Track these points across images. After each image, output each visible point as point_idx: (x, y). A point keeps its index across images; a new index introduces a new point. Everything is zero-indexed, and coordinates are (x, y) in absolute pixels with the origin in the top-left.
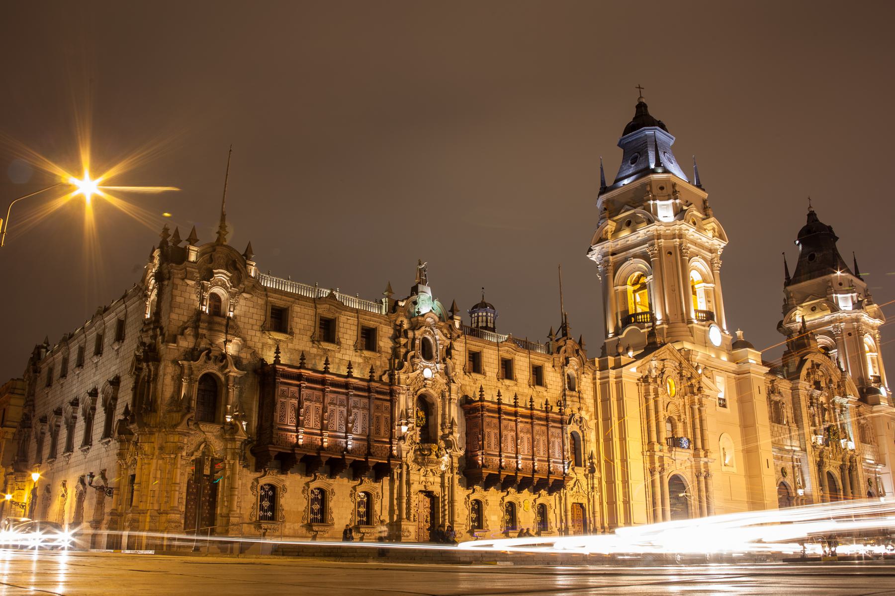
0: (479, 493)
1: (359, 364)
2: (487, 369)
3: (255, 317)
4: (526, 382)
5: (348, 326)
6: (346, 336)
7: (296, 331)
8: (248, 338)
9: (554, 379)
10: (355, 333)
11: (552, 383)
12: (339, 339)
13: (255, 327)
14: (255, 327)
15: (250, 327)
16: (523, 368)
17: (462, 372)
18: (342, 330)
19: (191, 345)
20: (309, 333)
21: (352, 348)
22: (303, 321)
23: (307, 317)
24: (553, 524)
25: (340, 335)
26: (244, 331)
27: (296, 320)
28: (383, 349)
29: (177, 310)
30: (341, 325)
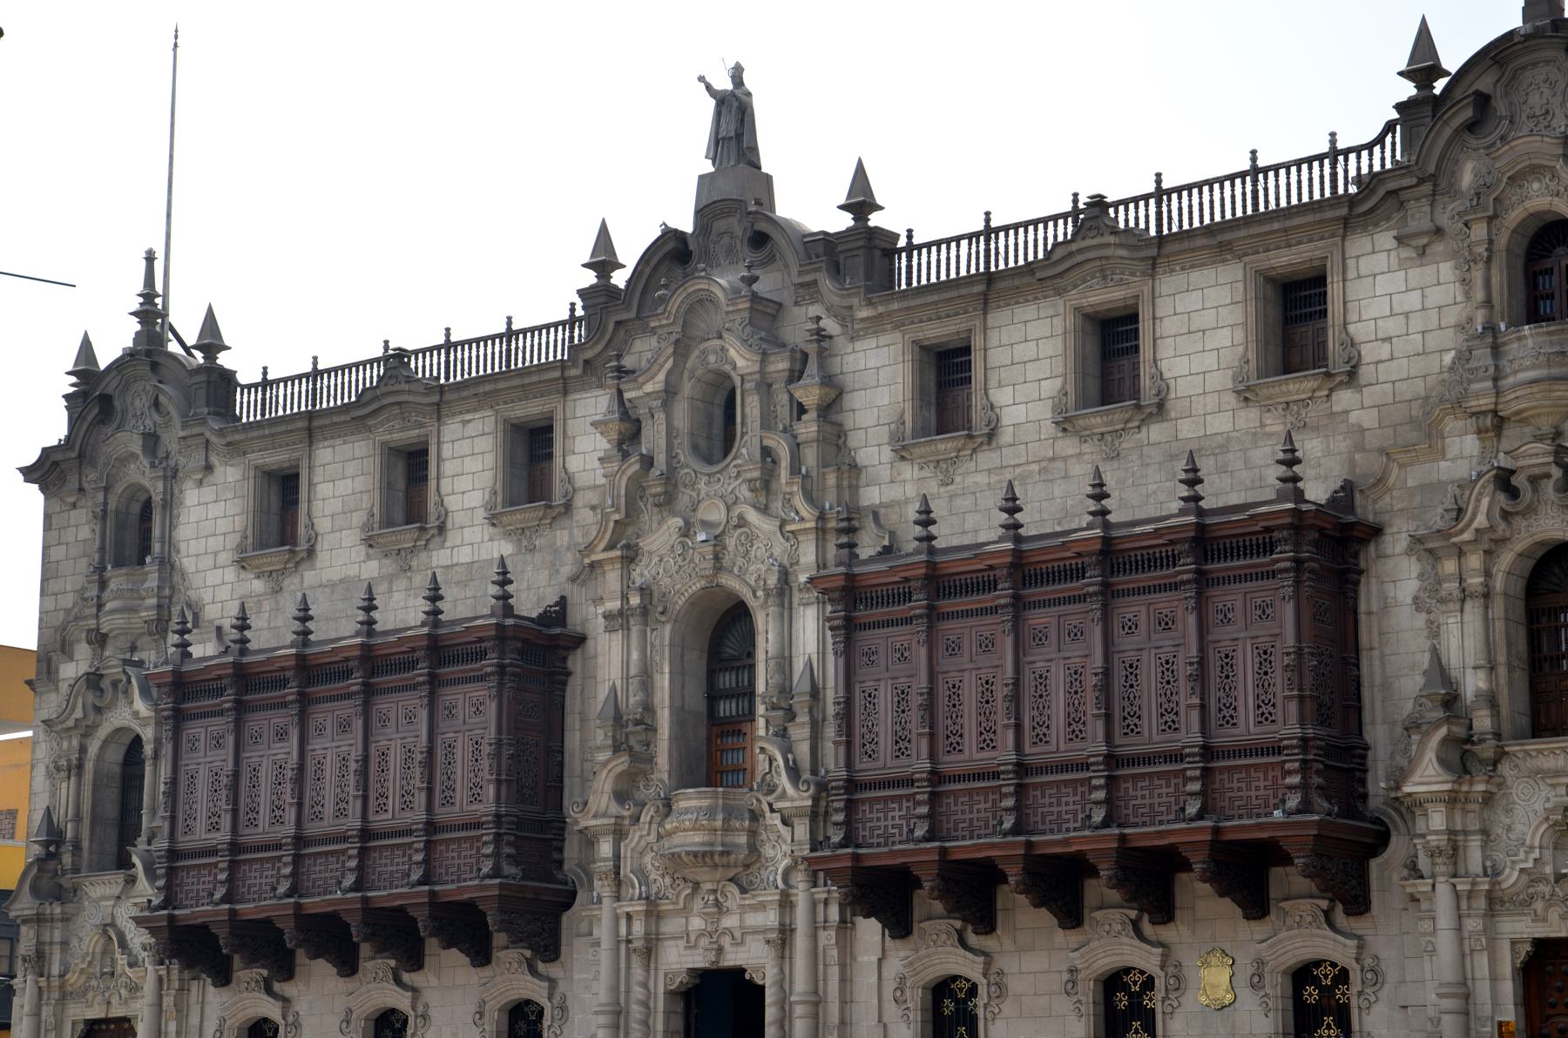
2: (1001, 396)
3: (223, 525)
4: (1222, 380)
7: (323, 525)
8: (207, 597)
10: (490, 460)
11: (1392, 327)
15: (209, 561)
16: (1207, 319)
17: (887, 453)
18: (449, 468)
20: (359, 518)
21: (481, 514)
23: (351, 468)
25: (446, 486)
26: (196, 581)
27: (323, 490)
29: (54, 586)
30: (447, 451)
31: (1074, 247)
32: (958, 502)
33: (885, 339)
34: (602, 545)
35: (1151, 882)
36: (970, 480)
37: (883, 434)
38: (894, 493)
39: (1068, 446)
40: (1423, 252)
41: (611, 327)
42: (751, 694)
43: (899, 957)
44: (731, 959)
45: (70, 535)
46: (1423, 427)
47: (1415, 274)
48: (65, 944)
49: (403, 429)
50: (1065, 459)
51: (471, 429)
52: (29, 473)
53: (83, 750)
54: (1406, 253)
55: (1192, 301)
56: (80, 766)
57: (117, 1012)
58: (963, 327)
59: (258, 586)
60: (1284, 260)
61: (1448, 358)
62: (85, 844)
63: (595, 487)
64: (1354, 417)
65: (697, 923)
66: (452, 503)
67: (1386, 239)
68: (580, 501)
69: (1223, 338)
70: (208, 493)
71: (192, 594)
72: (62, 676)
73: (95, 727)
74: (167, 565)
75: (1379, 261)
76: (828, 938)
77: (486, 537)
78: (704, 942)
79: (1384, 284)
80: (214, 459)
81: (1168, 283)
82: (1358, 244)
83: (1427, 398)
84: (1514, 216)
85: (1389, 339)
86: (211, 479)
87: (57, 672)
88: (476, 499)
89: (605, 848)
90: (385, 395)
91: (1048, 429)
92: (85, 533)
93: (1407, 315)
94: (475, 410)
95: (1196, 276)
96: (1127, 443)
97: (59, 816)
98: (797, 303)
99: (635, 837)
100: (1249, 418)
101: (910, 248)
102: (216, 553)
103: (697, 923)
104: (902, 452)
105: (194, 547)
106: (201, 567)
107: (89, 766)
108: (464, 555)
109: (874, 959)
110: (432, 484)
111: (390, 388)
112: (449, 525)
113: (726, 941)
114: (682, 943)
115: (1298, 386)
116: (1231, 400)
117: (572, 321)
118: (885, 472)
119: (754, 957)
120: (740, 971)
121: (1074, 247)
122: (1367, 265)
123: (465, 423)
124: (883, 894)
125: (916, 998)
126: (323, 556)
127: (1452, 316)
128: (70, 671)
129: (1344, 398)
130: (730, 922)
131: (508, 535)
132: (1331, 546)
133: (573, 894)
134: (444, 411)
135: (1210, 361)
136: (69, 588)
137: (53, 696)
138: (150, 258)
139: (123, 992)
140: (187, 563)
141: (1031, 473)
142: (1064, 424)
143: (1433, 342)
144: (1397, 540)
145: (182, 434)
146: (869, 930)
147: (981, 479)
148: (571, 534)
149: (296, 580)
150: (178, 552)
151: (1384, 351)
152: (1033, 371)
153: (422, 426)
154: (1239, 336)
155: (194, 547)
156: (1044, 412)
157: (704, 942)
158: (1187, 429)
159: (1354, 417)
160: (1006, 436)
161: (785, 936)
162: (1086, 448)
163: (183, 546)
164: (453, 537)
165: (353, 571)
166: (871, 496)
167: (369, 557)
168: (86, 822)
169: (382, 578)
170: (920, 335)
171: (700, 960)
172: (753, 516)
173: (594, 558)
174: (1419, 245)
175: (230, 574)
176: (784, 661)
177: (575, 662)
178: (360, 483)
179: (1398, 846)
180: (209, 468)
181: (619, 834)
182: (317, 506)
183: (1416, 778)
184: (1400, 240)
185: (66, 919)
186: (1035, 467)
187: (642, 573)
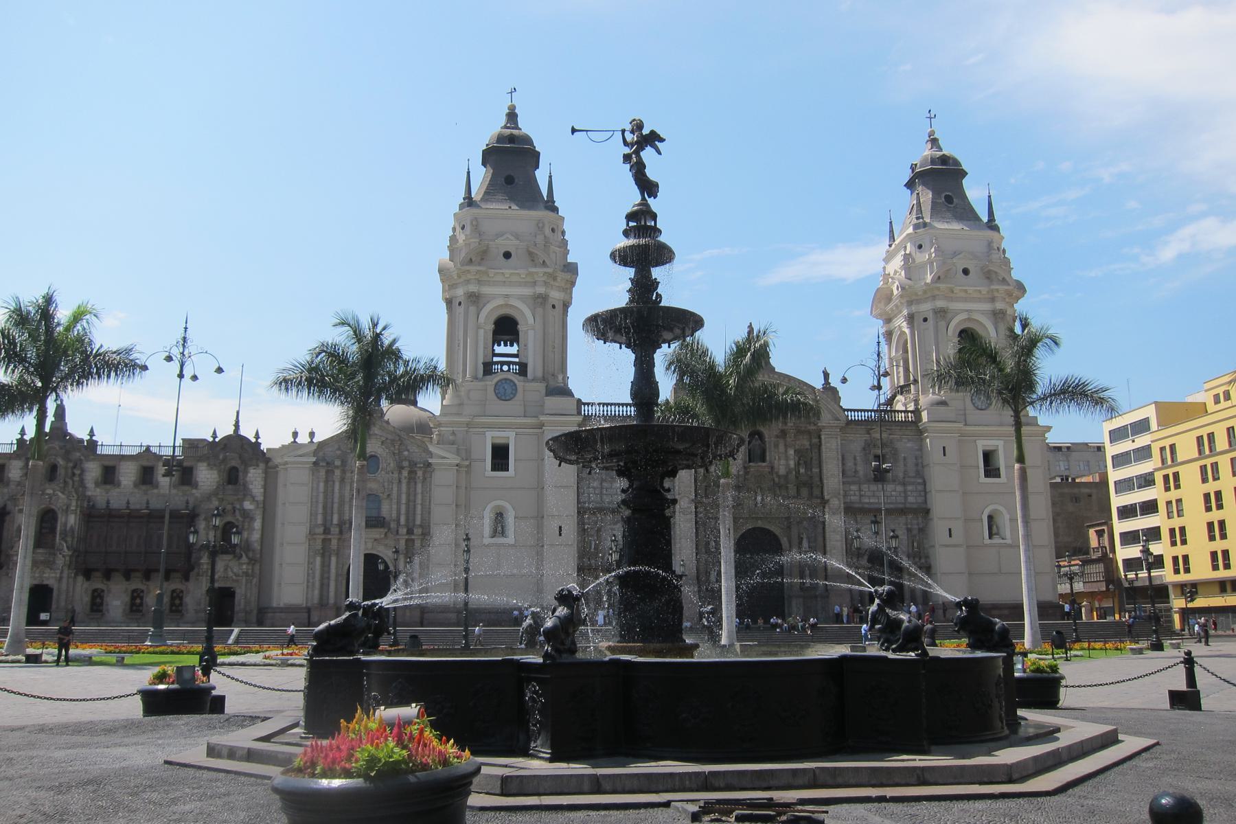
43: (86, 584)
46: (208, 498)
76: (71, 580)
104: (97, 484)
115: (186, 488)
119: (51, 582)
124: (88, 574)
125: (90, 592)
129: (194, 491)
132: (188, 518)
142: (136, 485)
144: (202, 517)
146: (80, 579)
156: (131, 484)
161: (61, 578)
174: (210, 466)
176: (66, 524)
177: (7, 518)
179: (196, 570)
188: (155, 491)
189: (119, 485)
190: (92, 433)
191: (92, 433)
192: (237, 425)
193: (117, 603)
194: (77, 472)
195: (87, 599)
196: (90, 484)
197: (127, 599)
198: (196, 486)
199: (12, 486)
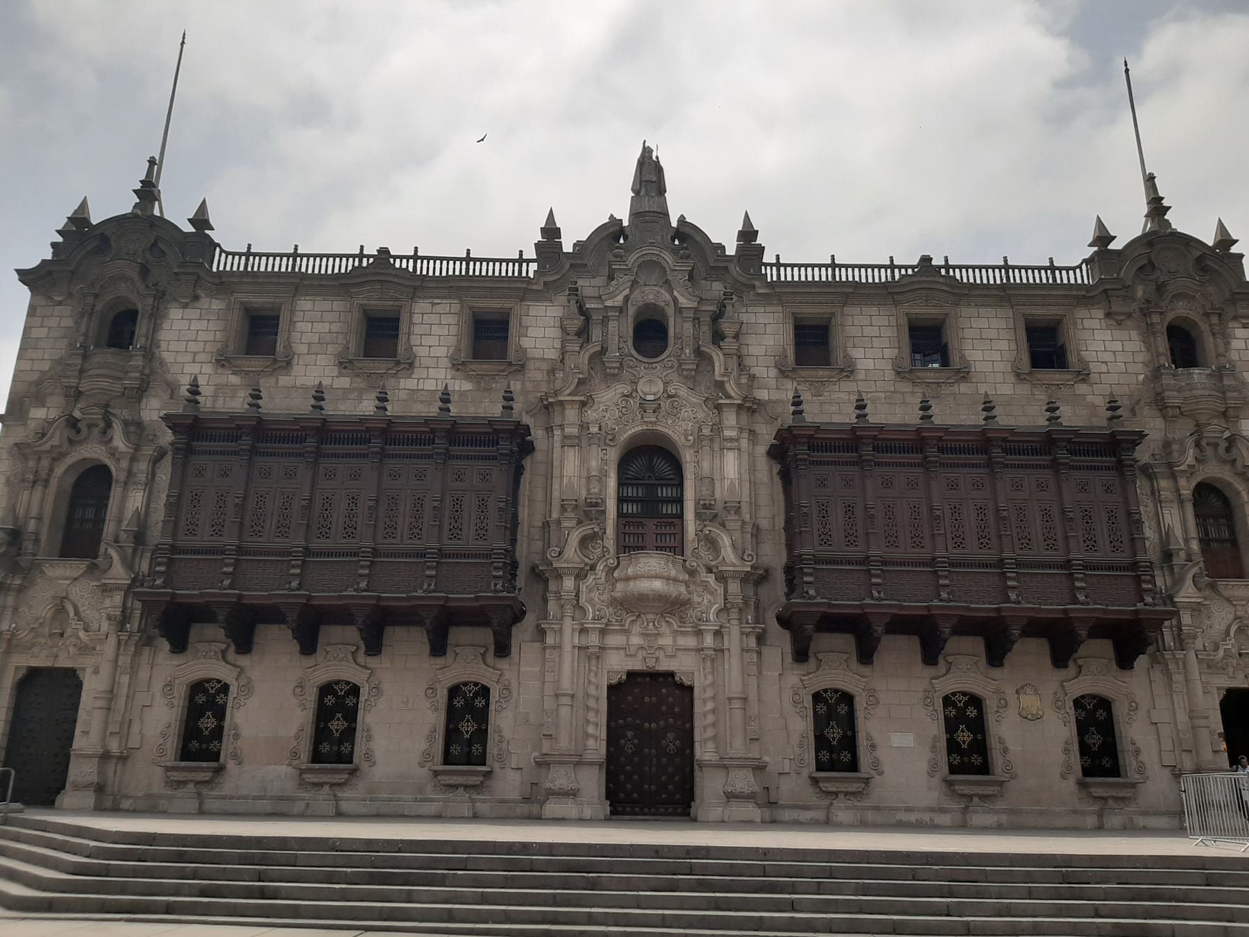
0: (836, 670)
1: (462, 394)
2: (857, 353)
3: (202, 336)
5: (434, 319)
6: (427, 341)
9: (1117, 346)
10: (454, 330)
11: (1108, 357)
12: (410, 348)
13: (201, 357)
14: (201, 357)
15: (189, 358)
16: (992, 334)
17: (773, 372)
18: (417, 329)
19: (53, 414)
20: (331, 348)
21: (445, 362)
22: (319, 327)
23: (329, 317)
24: (1150, 757)
25: (414, 340)
28: (530, 353)
29: (31, 354)
30: (417, 318)
31: (916, 279)
32: (826, 407)
33: (768, 309)
34: (568, 392)
35: (996, 642)
36: (835, 396)
37: (771, 361)
38: (775, 395)
39: (905, 387)
40: (1119, 323)
41: (567, 266)
42: (680, 501)
44: (664, 666)
45: (53, 322)
47: (1117, 333)
48: (15, 610)
49: (380, 299)
50: (903, 393)
51: (438, 309)
52: (25, 276)
53: (51, 470)
54: (1110, 322)
55: (983, 323)
56: (47, 481)
57: (64, 662)
58: (828, 311)
59: (234, 379)
60: (1040, 312)
61: (1141, 378)
62: (43, 538)
63: (543, 359)
64: (1089, 398)
65: (636, 640)
66: (420, 351)
67: (1099, 313)
68: (531, 365)
69: (1004, 345)
70: (192, 313)
71: (169, 377)
72: (31, 416)
73: (62, 456)
74: (150, 353)
75: (1095, 324)
77: (449, 376)
78: (641, 654)
79: (1098, 335)
80: (200, 293)
81: (965, 311)
82: (1081, 313)
83: (1131, 396)
84: (1170, 316)
85: (1106, 363)
86: (196, 305)
87: (27, 412)
88: (442, 352)
89: (569, 583)
90: (377, 274)
91: (890, 374)
92: (69, 322)
93: (1114, 352)
94: (445, 298)
95: (982, 310)
96: (946, 390)
97: (21, 512)
98: (705, 279)
99: (591, 579)
100: (1024, 389)
101: (778, 265)
102: (195, 353)
103: (636, 640)
104: (783, 373)
105: (174, 346)
106: (179, 359)
107: (54, 482)
108: (430, 385)
109: (777, 674)
110: (402, 338)
111: (378, 270)
112: (417, 364)
113: (661, 654)
114: (622, 652)
116: (1011, 378)
117: (521, 260)
118: (773, 383)
119: (683, 666)
120: (672, 674)
121: (916, 279)
122: (1087, 323)
123: (433, 304)
126: (297, 369)
127: (1141, 357)
128: (38, 414)
129: (1082, 388)
130: (666, 641)
131: (468, 378)
133: (524, 613)
134: (418, 294)
135: (997, 356)
136: (46, 357)
137: (21, 429)
138: (152, 162)
139: (71, 649)
140: (168, 357)
141: (879, 398)
143: (1131, 368)
145: (176, 270)
147: (841, 395)
148: (523, 384)
149: (272, 381)
150: (159, 347)
151: (1104, 369)
152: (876, 342)
153: (396, 299)
154: (1013, 346)
155: (174, 346)
157: (641, 654)
158: (983, 389)
159: (1089, 398)
160: (861, 375)
162: (916, 389)
163: (163, 345)
164: (418, 373)
165: (326, 382)
166: (763, 395)
167: (341, 375)
168: (46, 521)
169: (351, 390)
170: (797, 310)
171: (637, 665)
172: (683, 392)
173: (560, 398)
175: (208, 369)
177: (527, 463)
178: (336, 327)
180: (196, 298)
181: (580, 575)
182: (296, 336)
183: (1182, 593)
184: (1108, 315)
185: (21, 590)
186: (883, 395)
187: (591, 414)
188: (964, 388)
189: (848, 371)
190: (748, 234)
191: (748, 234)
192: (1157, 208)
193: (902, 740)
194: (727, 327)
195: (802, 726)
196: (765, 371)
197: (935, 728)
198: (1083, 375)
199: (536, 374)
